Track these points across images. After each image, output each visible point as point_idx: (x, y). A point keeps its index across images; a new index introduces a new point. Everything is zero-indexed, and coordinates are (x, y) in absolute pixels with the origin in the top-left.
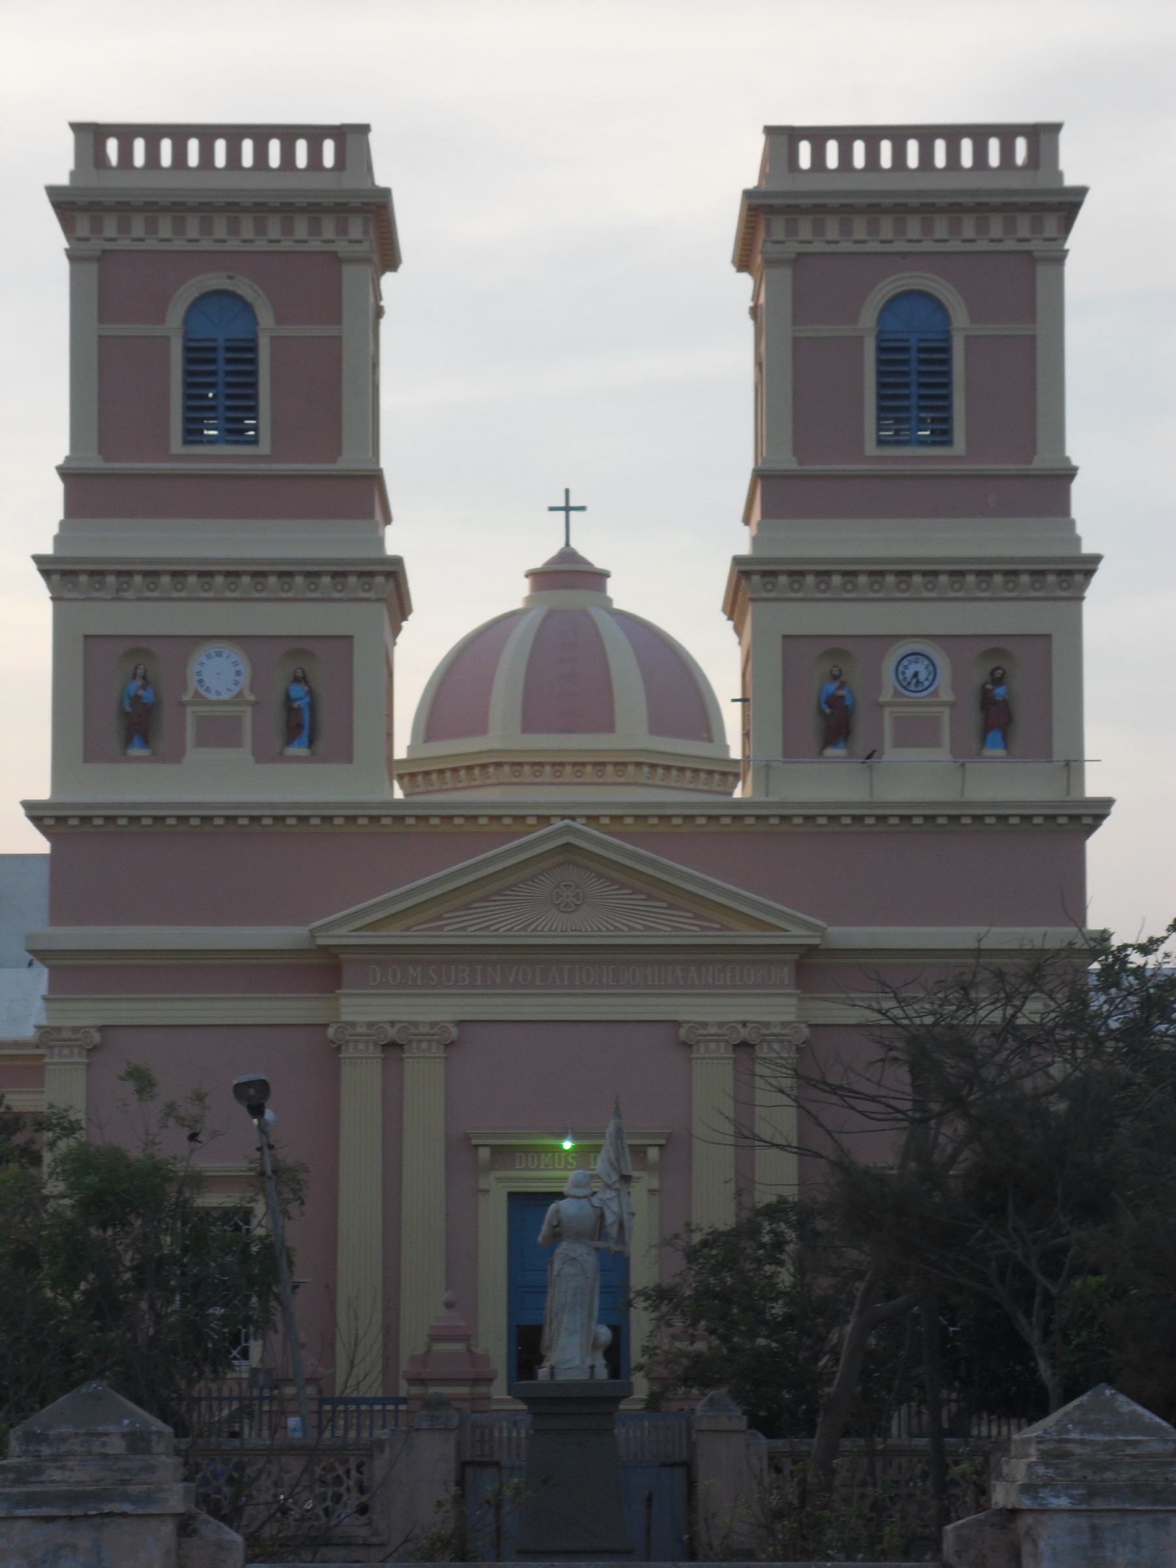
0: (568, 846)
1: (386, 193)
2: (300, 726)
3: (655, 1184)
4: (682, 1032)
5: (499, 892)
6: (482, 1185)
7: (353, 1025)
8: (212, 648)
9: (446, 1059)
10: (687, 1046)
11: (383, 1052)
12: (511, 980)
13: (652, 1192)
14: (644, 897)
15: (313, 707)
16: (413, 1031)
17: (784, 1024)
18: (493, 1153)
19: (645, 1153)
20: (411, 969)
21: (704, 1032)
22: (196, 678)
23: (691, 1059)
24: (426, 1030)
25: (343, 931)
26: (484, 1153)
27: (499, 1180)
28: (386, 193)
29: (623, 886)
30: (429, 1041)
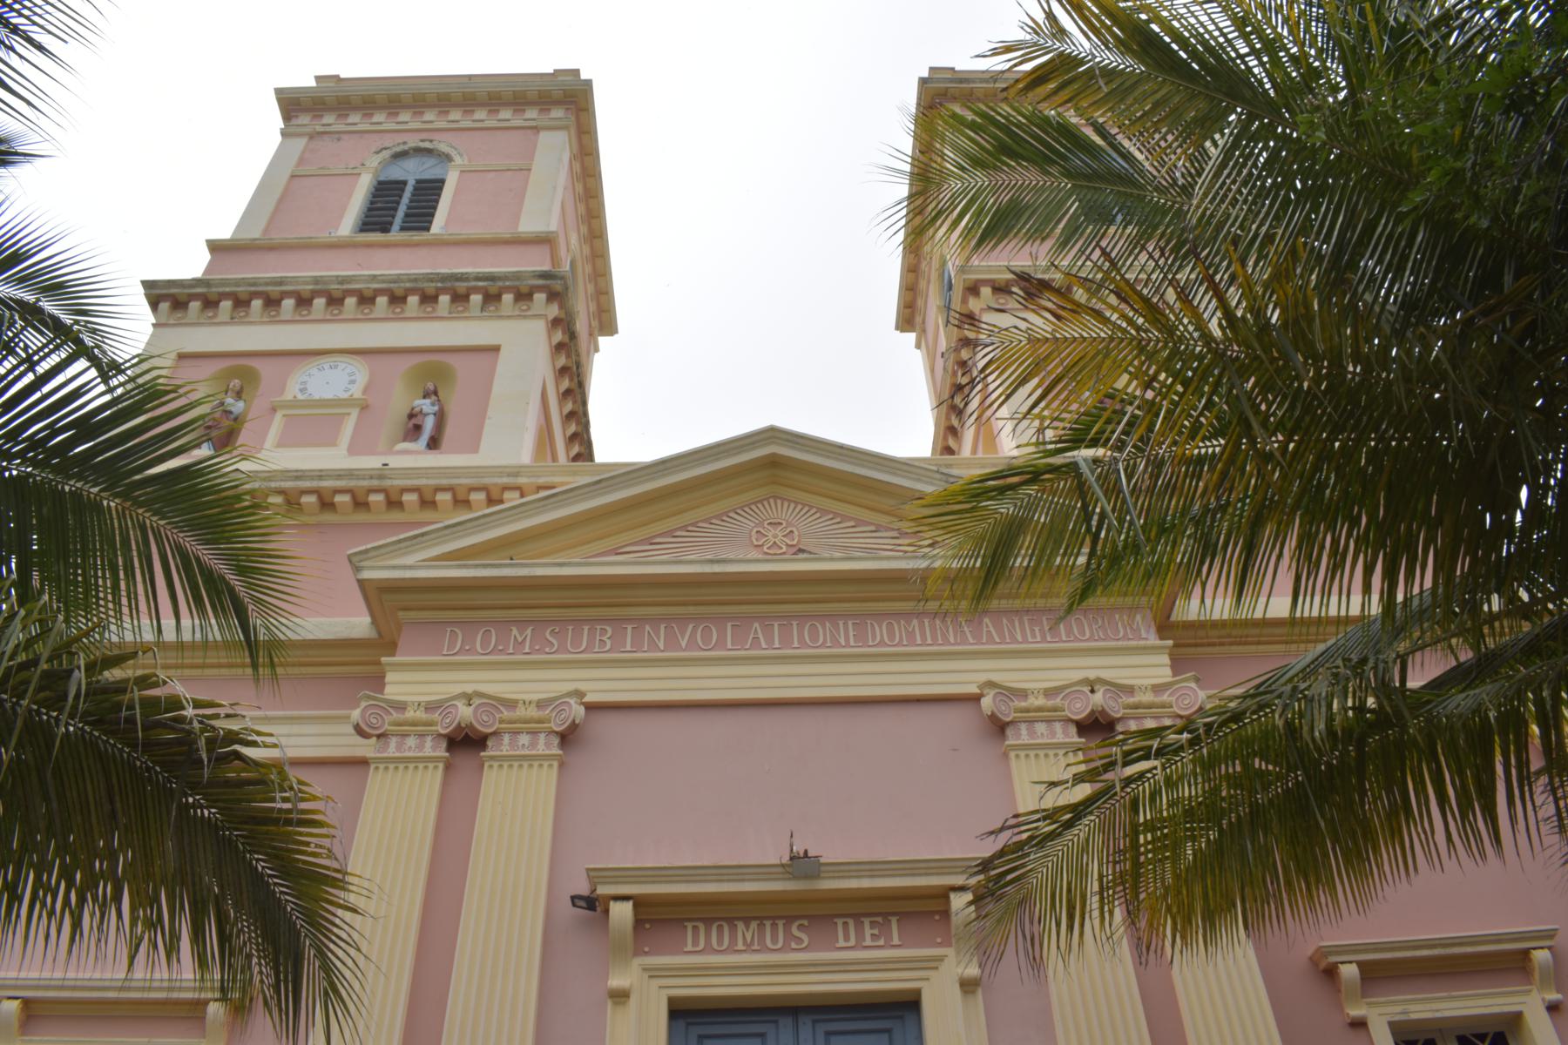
0: (774, 462)
1: (589, 83)
2: (418, 428)
3: (973, 971)
4: (987, 703)
6: (616, 981)
7: (401, 707)
8: (326, 361)
9: (562, 765)
10: (999, 727)
11: (449, 749)
12: (684, 644)
13: (968, 986)
14: (895, 534)
15: (441, 418)
16: (506, 714)
17: (1158, 689)
18: (639, 923)
19: (946, 913)
20: (515, 631)
21: (1023, 704)
22: (298, 386)
23: (1005, 755)
24: (532, 712)
25: (410, 560)
26: (622, 913)
27: (653, 973)
28: (589, 83)
30: (534, 733)
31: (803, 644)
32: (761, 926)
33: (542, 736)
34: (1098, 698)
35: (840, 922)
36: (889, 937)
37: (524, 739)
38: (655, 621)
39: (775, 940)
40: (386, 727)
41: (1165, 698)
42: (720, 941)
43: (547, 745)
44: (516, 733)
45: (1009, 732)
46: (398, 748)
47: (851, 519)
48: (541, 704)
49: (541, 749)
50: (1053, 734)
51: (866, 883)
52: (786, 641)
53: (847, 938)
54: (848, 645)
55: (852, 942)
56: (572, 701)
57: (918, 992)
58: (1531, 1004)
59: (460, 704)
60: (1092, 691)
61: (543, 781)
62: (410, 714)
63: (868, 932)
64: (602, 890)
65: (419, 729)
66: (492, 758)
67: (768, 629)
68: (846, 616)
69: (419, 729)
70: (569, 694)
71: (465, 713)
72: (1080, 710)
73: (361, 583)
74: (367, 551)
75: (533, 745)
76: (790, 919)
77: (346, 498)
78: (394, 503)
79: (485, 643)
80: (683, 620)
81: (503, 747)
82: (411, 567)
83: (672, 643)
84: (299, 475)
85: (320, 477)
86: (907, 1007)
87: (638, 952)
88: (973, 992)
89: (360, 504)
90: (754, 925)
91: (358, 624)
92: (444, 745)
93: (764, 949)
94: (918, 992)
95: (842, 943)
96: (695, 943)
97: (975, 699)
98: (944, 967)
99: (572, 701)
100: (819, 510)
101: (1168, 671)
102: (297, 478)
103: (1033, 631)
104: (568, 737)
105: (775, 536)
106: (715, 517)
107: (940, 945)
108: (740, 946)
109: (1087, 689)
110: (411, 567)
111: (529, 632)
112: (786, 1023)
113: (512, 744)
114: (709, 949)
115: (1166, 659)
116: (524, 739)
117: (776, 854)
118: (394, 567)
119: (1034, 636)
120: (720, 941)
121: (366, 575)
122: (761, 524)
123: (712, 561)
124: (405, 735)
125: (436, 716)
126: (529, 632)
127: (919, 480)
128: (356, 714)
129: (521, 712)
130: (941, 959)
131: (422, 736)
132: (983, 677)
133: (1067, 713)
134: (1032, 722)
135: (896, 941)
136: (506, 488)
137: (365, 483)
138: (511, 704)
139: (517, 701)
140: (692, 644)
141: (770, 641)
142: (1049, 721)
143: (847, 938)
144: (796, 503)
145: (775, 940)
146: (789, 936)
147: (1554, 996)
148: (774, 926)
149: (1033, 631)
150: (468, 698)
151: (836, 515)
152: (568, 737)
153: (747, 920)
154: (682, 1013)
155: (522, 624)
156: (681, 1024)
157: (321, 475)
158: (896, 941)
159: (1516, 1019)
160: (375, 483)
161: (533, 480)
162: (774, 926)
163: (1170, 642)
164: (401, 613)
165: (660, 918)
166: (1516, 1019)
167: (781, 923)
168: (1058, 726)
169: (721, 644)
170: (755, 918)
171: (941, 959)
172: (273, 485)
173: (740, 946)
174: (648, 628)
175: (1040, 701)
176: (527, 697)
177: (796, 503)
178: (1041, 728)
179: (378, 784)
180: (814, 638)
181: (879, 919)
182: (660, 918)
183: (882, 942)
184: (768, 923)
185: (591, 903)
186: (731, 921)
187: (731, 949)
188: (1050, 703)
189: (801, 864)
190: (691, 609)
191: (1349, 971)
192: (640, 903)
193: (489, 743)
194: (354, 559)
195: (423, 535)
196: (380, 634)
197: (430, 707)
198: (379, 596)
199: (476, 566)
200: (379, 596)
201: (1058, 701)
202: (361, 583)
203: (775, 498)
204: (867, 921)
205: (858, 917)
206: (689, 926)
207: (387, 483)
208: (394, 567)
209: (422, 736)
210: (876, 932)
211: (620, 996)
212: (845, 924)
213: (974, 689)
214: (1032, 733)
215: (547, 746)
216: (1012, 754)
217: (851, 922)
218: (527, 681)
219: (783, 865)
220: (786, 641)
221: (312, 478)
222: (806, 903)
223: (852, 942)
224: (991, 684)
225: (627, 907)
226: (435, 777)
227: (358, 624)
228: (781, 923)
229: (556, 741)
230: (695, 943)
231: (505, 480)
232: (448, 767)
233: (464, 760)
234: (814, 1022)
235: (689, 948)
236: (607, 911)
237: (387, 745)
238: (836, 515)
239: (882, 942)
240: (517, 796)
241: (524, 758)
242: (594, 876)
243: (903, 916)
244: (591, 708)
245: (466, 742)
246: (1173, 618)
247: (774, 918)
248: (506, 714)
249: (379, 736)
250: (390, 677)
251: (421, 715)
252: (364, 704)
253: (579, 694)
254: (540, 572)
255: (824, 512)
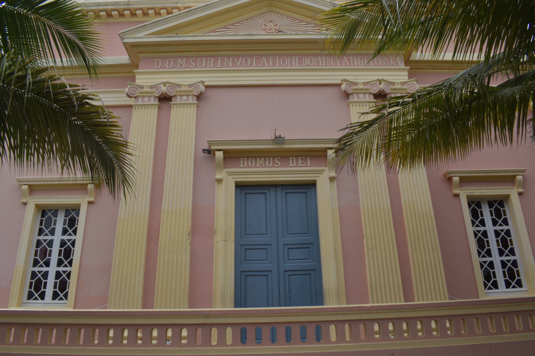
3: (333, 174)
4: (343, 87)
5: (233, 25)
6: (218, 176)
7: (142, 87)
9: (198, 106)
10: (347, 95)
12: (238, 65)
13: (332, 179)
16: (178, 89)
17: (403, 84)
18: (225, 158)
19: (326, 156)
20: (179, 60)
21: (356, 87)
23: (349, 105)
24: (187, 89)
25: (141, 35)
26: (219, 155)
29: (301, 21)
30: (188, 96)
31: (280, 65)
32: (265, 159)
33: (191, 97)
34: (382, 86)
35: (291, 158)
36: (307, 164)
37: (184, 98)
38: (228, 57)
39: (269, 164)
40: (137, 94)
41: (405, 87)
42: (252, 164)
43: (193, 100)
44: (182, 96)
45: (350, 97)
46: (142, 101)
47: (298, 20)
48: (190, 86)
49: (190, 101)
50: (365, 98)
51: (300, 146)
52: (274, 64)
53: (293, 164)
54: (296, 66)
55: (295, 165)
56: (200, 85)
57: (315, 181)
58: (513, 193)
59: (162, 86)
60: (380, 84)
61: (192, 112)
62: (145, 90)
63: (300, 162)
64: (213, 148)
65: (148, 95)
66: (174, 104)
67: (268, 60)
68: (295, 55)
69: (148, 95)
70: (199, 82)
71: (164, 89)
72: (375, 90)
73: (124, 44)
74: (125, 32)
75: (188, 100)
76: (274, 157)
77: (116, 13)
78: (133, 14)
79: (169, 65)
80: (238, 56)
81: (178, 100)
82: (141, 38)
83: (234, 64)
84: (99, 4)
85: (106, 5)
86: (312, 185)
87: (225, 167)
88: (333, 181)
89: (121, 15)
90: (263, 159)
91: (124, 58)
92: (157, 100)
93: (266, 166)
94: (315, 181)
95: (291, 165)
96: (244, 164)
97: (339, 85)
98: (324, 173)
99: (200, 85)
100: (287, 16)
101: (407, 78)
102: (98, 6)
103: (361, 62)
104: (199, 97)
105: (271, 26)
106: (249, 19)
107: (323, 166)
108: (258, 166)
109: (378, 83)
110: (141, 38)
111: (184, 60)
112: (273, 190)
113: (181, 99)
114: (248, 166)
115: (406, 73)
116: (184, 98)
117: (270, 136)
118: (136, 38)
119: (361, 64)
120: (252, 164)
121: (126, 41)
122: (265, 21)
123: (248, 35)
124: (144, 97)
125: (154, 90)
126: (184, 60)
127: (323, 5)
128: (127, 90)
129: (183, 88)
130: (323, 171)
131: (150, 97)
132: (343, 78)
133: (371, 91)
134: (358, 94)
135: (309, 165)
136: (173, 8)
137: (123, 7)
138: (179, 86)
139: (181, 85)
140: (241, 65)
141: (269, 64)
142: (364, 94)
143: (293, 164)
144: (279, 14)
145: (269, 164)
146: (274, 163)
147: (521, 190)
148: (269, 159)
149: (361, 62)
150: (165, 84)
151: (293, 18)
152: (199, 97)
153: (260, 157)
154: (240, 186)
155: (182, 57)
156: (239, 189)
157: (106, 4)
158: (309, 165)
159: (508, 197)
160: (126, 7)
161: (183, 5)
162: (269, 159)
163: (409, 67)
164: (139, 54)
165: (232, 156)
166: (508, 197)
167: (271, 159)
168: (367, 95)
169: (251, 65)
170: (263, 157)
171: (323, 171)
172: (89, 8)
173: (258, 166)
174: (226, 59)
175: (362, 87)
176: (185, 83)
177: (279, 14)
178: (361, 96)
179: (136, 113)
180: (284, 63)
181: (304, 158)
182: (232, 156)
183: (304, 165)
184: (267, 159)
185: (209, 152)
186: (255, 158)
187: (255, 167)
188: (365, 87)
189: (278, 139)
190: (241, 52)
191: (456, 179)
192: (225, 152)
193: (173, 99)
194: (121, 35)
195: (145, 26)
196: (132, 62)
197: (152, 87)
198: (131, 48)
199: (164, 37)
200: (131, 48)
201: (368, 87)
202: (124, 44)
203: (271, 11)
204: (300, 158)
205: (297, 157)
206: (242, 159)
207: (130, 7)
208: (136, 38)
209: (150, 97)
210: (302, 162)
211: (220, 181)
212: (293, 159)
213: (339, 82)
214: (358, 98)
215: (192, 100)
216: (351, 105)
217: (294, 159)
218: (185, 77)
219: (272, 140)
220: (274, 64)
221: (103, 5)
222: (280, 152)
223: (295, 165)
224: (345, 80)
225: (221, 153)
226: (155, 111)
227: (124, 58)
228: (271, 159)
229: (195, 98)
230: (244, 164)
231: (173, 5)
232: (159, 107)
233: (165, 105)
234: (282, 189)
235: (242, 166)
236: (214, 154)
237: (138, 101)
238: (293, 18)
239: (304, 165)
240: (183, 118)
241: (185, 104)
242: (210, 143)
243: (312, 157)
244: (207, 87)
245: (165, 99)
246: (411, 59)
247: (269, 157)
248: (178, 89)
249: (135, 97)
250: (137, 77)
251: (149, 90)
252: (129, 86)
253: (203, 82)
254: (187, 39)
255: (288, 17)
